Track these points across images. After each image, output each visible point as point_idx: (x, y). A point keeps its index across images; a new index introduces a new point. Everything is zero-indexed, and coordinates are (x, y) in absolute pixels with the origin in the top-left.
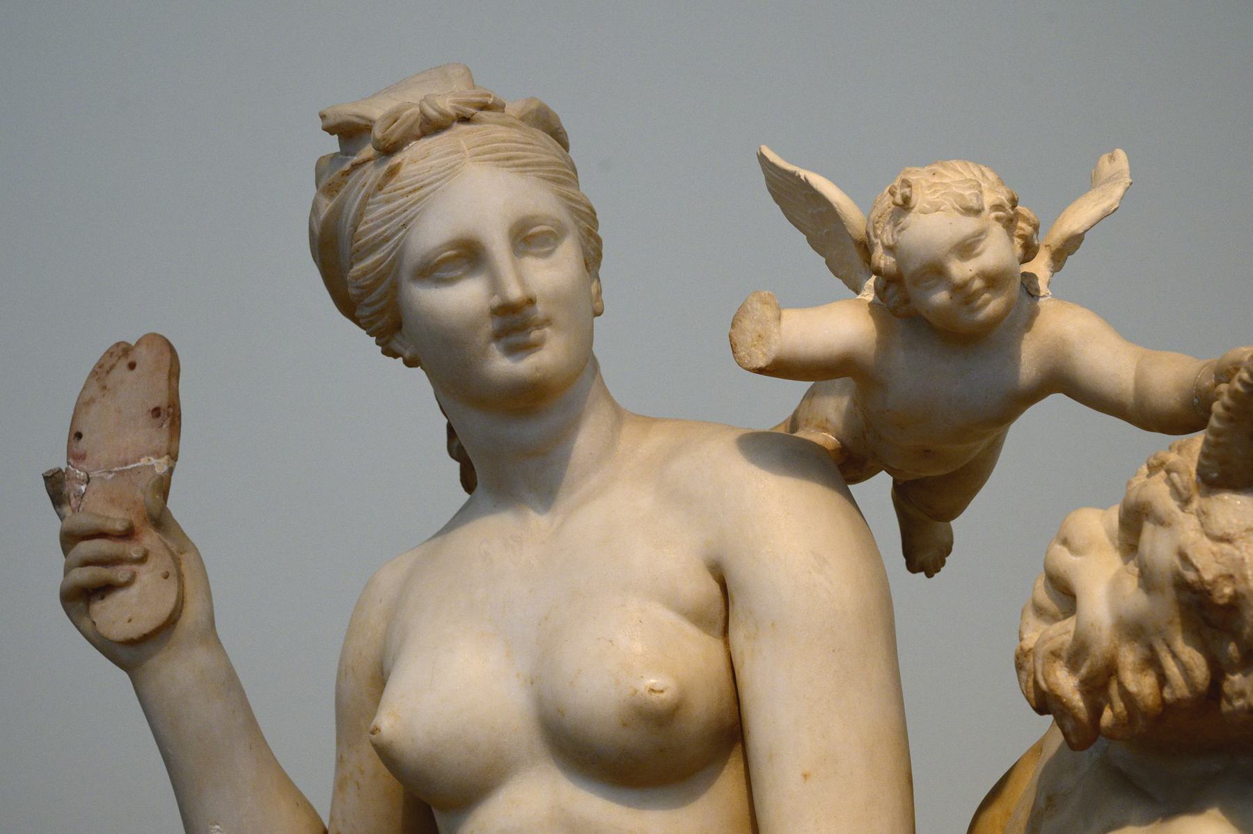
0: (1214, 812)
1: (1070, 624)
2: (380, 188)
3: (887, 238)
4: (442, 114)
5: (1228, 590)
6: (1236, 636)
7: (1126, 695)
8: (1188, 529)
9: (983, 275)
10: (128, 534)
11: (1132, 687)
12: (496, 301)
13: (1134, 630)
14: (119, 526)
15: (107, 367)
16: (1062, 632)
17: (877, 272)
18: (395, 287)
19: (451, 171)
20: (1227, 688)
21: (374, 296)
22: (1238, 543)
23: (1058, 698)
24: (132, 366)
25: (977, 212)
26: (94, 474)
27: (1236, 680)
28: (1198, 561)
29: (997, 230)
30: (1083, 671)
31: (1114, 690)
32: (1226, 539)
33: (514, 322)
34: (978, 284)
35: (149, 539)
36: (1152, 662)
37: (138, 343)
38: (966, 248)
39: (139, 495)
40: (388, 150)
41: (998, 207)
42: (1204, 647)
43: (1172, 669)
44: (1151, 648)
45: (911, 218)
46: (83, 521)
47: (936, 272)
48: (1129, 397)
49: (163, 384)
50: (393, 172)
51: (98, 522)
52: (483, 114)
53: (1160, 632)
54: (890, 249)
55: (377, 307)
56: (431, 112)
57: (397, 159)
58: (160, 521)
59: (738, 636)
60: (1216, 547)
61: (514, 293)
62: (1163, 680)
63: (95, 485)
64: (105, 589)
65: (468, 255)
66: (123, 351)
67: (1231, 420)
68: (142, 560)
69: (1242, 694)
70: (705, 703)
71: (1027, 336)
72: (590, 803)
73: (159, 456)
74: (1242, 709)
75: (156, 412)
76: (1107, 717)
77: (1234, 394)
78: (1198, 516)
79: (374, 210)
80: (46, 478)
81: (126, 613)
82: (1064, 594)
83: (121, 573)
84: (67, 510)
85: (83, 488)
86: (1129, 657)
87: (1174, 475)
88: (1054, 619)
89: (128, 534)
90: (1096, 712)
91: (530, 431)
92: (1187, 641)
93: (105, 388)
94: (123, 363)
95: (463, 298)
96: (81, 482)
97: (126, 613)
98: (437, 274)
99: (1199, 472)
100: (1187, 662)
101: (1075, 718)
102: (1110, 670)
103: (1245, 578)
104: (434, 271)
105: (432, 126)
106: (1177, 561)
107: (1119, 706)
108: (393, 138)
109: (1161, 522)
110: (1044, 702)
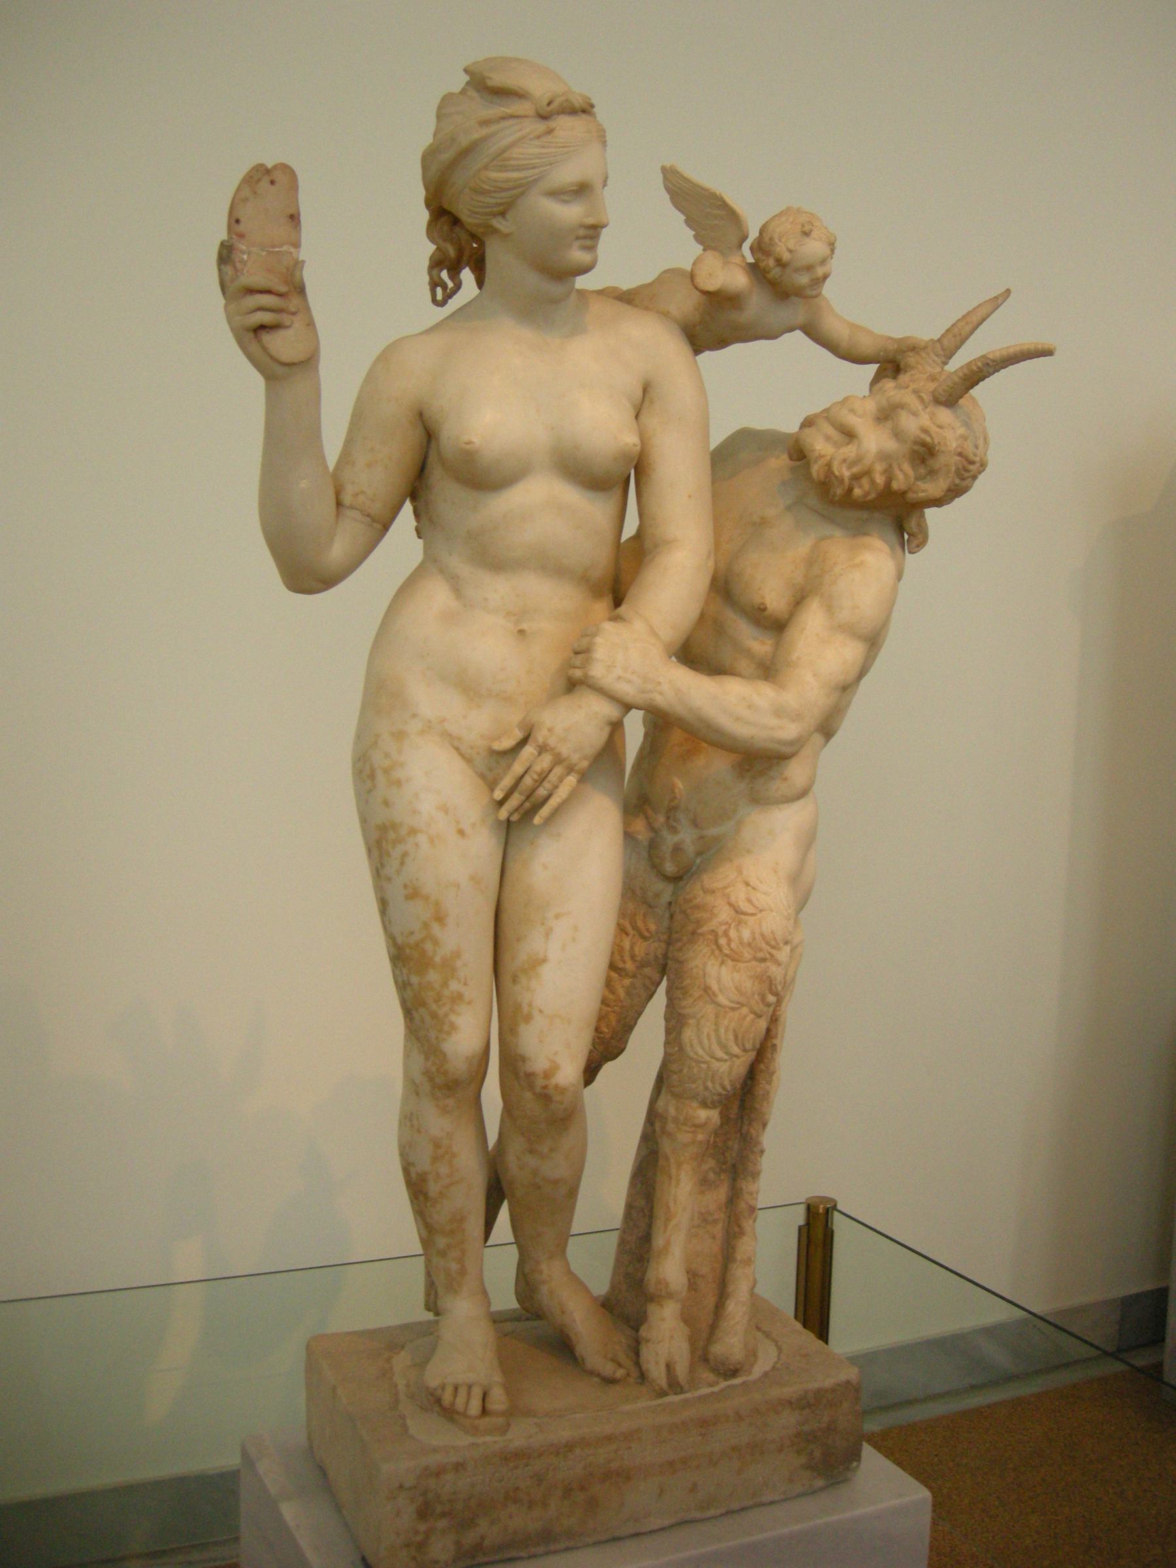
2: (539, 137)
3: (791, 245)
7: (873, 482)
8: (925, 420)
11: (878, 481)
12: (590, 221)
13: (883, 456)
14: (283, 289)
16: (850, 451)
18: (523, 193)
21: (503, 194)
24: (272, 182)
27: (922, 485)
28: (934, 435)
30: (855, 470)
31: (865, 482)
32: (941, 427)
35: (294, 303)
37: (275, 167)
39: (284, 271)
42: (913, 467)
43: (900, 476)
44: (890, 466)
45: (806, 240)
47: (809, 268)
50: (550, 131)
55: (499, 201)
57: (551, 124)
58: (301, 290)
59: (652, 421)
60: (938, 430)
66: (268, 171)
68: (294, 314)
69: (923, 491)
72: (571, 495)
75: (292, 217)
76: (857, 492)
83: (286, 319)
84: (229, 270)
85: (245, 257)
86: (879, 467)
88: (837, 445)
90: (850, 490)
91: (556, 289)
93: (255, 193)
95: (571, 213)
96: (243, 253)
97: (283, 344)
98: (563, 197)
102: (868, 473)
103: (945, 444)
106: (918, 432)
107: (867, 486)
109: (915, 414)
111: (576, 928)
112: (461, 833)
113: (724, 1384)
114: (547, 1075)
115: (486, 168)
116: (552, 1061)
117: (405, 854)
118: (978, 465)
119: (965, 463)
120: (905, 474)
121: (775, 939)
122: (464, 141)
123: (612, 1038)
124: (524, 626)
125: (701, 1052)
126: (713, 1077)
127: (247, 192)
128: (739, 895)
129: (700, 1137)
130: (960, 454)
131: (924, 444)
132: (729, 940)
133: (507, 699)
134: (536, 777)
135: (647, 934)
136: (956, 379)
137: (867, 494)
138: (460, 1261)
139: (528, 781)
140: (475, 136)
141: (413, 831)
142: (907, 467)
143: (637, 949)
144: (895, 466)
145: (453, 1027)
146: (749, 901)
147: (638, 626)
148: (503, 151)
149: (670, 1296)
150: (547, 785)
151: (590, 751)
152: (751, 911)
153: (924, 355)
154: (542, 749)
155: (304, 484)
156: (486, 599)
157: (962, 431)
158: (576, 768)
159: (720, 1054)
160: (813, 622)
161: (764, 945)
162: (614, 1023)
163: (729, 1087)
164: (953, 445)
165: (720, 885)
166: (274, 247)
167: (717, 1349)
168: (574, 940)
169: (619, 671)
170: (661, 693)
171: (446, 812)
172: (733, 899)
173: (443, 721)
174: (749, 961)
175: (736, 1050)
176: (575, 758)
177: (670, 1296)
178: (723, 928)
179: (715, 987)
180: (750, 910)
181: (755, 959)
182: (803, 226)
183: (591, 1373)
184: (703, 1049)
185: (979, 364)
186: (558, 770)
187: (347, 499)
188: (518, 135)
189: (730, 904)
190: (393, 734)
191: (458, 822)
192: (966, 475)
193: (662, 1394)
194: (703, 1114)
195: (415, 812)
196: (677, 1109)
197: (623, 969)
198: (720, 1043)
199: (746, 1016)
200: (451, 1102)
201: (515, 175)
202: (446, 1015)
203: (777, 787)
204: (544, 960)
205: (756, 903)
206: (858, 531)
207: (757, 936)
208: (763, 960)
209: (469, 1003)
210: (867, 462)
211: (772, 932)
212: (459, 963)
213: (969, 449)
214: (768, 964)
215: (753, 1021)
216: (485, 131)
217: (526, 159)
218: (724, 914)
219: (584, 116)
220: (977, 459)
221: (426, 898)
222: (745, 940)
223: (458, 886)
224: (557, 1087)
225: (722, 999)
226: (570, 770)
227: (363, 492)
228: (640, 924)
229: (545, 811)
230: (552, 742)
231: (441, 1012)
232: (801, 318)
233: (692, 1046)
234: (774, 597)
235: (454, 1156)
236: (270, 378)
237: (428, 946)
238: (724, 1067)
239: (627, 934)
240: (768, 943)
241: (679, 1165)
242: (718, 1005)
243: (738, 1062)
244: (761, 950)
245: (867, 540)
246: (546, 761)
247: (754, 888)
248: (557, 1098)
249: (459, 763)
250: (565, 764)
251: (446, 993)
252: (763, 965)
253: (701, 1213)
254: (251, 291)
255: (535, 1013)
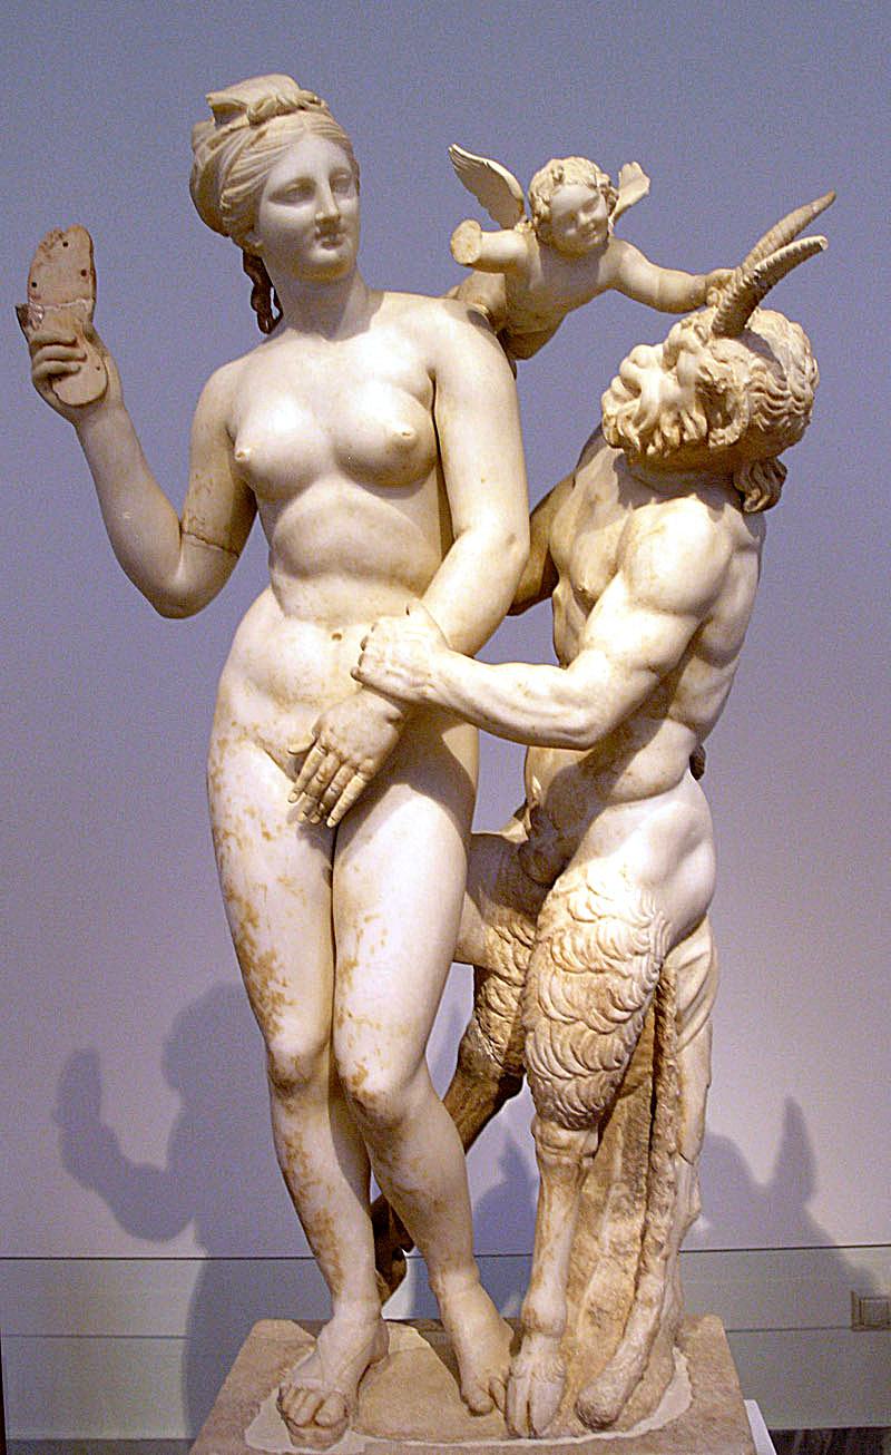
0: (694, 496)
1: (637, 402)
2: (252, 144)
3: (547, 198)
4: (291, 103)
5: (723, 387)
6: (721, 411)
7: (663, 437)
8: (707, 359)
9: (593, 221)
10: (73, 344)
11: (668, 434)
12: (320, 216)
13: (671, 406)
15: (49, 244)
16: (634, 406)
17: (539, 215)
18: (257, 203)
19: (297, 138)
20: (712, 435)
22: (731, 363)
23: (629, 439)
24: (65, 245)
25: (593, 187)
26: (46, 308)
27: (720, 432)
29: (602, 197)
30: (642, 426)
33: (329, 229)
34: (592, 226)
35: (85, 347)
36: (679, 422)
38: (588, 206)
40: (256, 122)
41: (603, 186)
42: (706, 415)
43: (689, 424)
44: (679, 414)
45: (560, 187)
46: (45, 332)
47: (572, 218)
48: (656, 295)
49: (88, 257)
50: (261, 135)
51: (55, 335)
52: (312, 105)
53: (684, 407)
54: (547, 203)
56: (284, 101)
57: (263, 128)
61: (333, 211)
62: (683, 429)
63: (47, 314)
64: (64, 374)
65: (304, 189)
67: (736, 301)
68: (84, 359)
69: (723, 438)
70: (427, 444)
71: (603, 258)
73: (86, 298)
74: (723, 445)
76: (651, 450)
77: (740, 289)
78: (710, 349)
79: (244, 158)
80: (17, 309)
81: (73, 391)
82: (635, 390)
83: (73, 366)
84: (29, 329)
86: (667, 419)
87: (700, 329)
89: (73, 344)
90: (645, 447)
92: (697, 410)
93: (49, 256)
94: (60, 244)
95: (299, 214)
96: (39, 312)
97: (73, 391)
99: (713, 329)
100: (696, 421)
101: (635, 449)
102: (656, 426)
104: (283, 197)
105: (286, 110)
107: (659, 442)
108: (263, 115)
110: (622, 442)
111: (385, 932)
112: (267, 835)
113: (591, 1436)
114: (355, 1083)
115: (224, 188)
116: (361, 1067)
117: (223, 857)
118: (792, 399)
119: (769, 398)
120: (695, 423)
121: (616, 950)
122: (202, 167)
123: (509, 1050)
124: (340, 631)
125: (542, 1067)
126: (559, 1095)
127: (42, 257)
128: (578, 901)
129: (565, 1160)
130: (759, 390)
131: (705, 384)
132: (563, 948)
133: (312, 703)
134: (321, 778)
135: (529, 942)
136: (727, 303)
137: (664, 449)
138: (336, 1265)
139: (314, 782)
140: (207, 159)
141: (227, 834)
142: (695, 414)
143: (520, 960)
144: (683, 414)
145: (276, 1025)
146: (588, 906)
147: (418, 615)
148: (231, 166)
149: (539, 1329)
150: (333, 785)
151: (370, 749)
152: (586, 918)
153: (728, 287)
154: (327, 750)
155: (126, 516)
156: (298, 607)
157: (759, 362)
158: (360, 768)
159: (562, 1072)
160: (614, 597)
161: (600, 954)
162: (509, 1034)
163: (583, 1109)
164: (746, 380)
165: (562, 890)
166: (67, 302)
167: (587, 1397)
168: (382, 943)
169: (389, 666)
170: (432, 686)
171: (253, 815)
172: (572, 907)
173: (256, 728)
174: (583, 972)
175: (579, 1069)
176: (357, 757)
177: (539, 1329)
178: (560, 934)
179: (547, 999)
180: (586, 915)
181: (590, 970)
182: (553, 172)
183: (465, 1400)
184: (544, 1064)
185: (747, 280)
186: (344, 770)
187: (186, 528)
188: (240, 146)
189: (569, 910)
190: (218, 743)
191: (263, 825)
192: (776, 413)
193: (515, 1435)
194: (564, 1136)
195: (228, 816)
196: (542, 1132)
197: (509, 978)
198: (558, 1060)
199: (583, 1033)
200: (291, 1102)
201: (241, 188)
202: (270, 1015)
203: (624, 784)
204: (354, 964)
205: (595, 909)
206: (668, 494)
207: (592, 944)
208: (602, 971)
209: (291, 1004)
210: (651, 416)
211: (612, 941)
212: (275, 964)
213: (770, 380)
214: (607, 975)
215: (594, 1038)
216: (214, 152)
217: (241, 170)
218: (562, 919)
219: (302, 112)
220: (788, 392)
221: (239, 900)
222: (579, 949)
223: (266, 888)
224: (365, 1093)
225: (553, 1012)
226: (356, 769)
227: (194, 518)
228: (519, 932)
229: (335, 813)
230: (333, 743)
231: (266, 1013)
232: (603, 274)
233: (533, 1060)
234: (588, 582)
235: (304, 1155)
236: (72, 421)
237: (247, 947)
238: (570, 1087)
239: (509, 942)
240: (605, 953)
241: (551, 1187)
242: (551, 1019)
243: (586, 1081)
244: (596, 960)
245: (680, 502)
246: (331, 757)
247: (595, 893)
248: (369, 1105)
249: (275, 768)
250: (350, 763)
251: (267, 993)
252: (600, 976)
253: (612, 1242)
254: (41, 344)
255: (346, 1017)
